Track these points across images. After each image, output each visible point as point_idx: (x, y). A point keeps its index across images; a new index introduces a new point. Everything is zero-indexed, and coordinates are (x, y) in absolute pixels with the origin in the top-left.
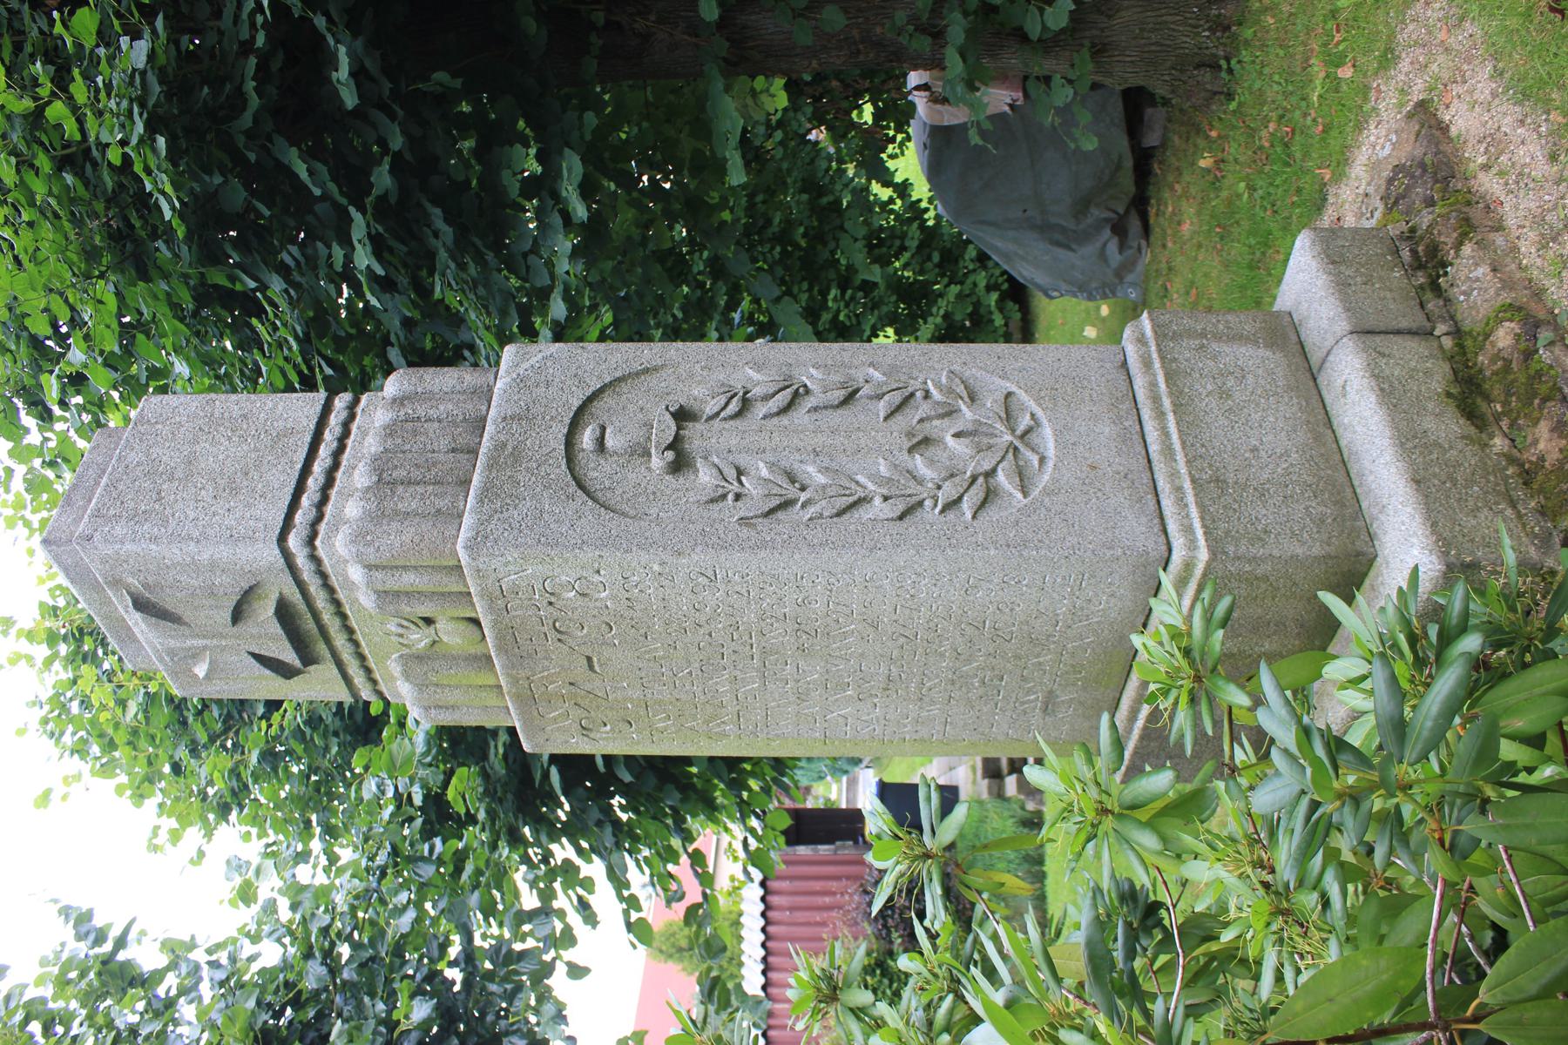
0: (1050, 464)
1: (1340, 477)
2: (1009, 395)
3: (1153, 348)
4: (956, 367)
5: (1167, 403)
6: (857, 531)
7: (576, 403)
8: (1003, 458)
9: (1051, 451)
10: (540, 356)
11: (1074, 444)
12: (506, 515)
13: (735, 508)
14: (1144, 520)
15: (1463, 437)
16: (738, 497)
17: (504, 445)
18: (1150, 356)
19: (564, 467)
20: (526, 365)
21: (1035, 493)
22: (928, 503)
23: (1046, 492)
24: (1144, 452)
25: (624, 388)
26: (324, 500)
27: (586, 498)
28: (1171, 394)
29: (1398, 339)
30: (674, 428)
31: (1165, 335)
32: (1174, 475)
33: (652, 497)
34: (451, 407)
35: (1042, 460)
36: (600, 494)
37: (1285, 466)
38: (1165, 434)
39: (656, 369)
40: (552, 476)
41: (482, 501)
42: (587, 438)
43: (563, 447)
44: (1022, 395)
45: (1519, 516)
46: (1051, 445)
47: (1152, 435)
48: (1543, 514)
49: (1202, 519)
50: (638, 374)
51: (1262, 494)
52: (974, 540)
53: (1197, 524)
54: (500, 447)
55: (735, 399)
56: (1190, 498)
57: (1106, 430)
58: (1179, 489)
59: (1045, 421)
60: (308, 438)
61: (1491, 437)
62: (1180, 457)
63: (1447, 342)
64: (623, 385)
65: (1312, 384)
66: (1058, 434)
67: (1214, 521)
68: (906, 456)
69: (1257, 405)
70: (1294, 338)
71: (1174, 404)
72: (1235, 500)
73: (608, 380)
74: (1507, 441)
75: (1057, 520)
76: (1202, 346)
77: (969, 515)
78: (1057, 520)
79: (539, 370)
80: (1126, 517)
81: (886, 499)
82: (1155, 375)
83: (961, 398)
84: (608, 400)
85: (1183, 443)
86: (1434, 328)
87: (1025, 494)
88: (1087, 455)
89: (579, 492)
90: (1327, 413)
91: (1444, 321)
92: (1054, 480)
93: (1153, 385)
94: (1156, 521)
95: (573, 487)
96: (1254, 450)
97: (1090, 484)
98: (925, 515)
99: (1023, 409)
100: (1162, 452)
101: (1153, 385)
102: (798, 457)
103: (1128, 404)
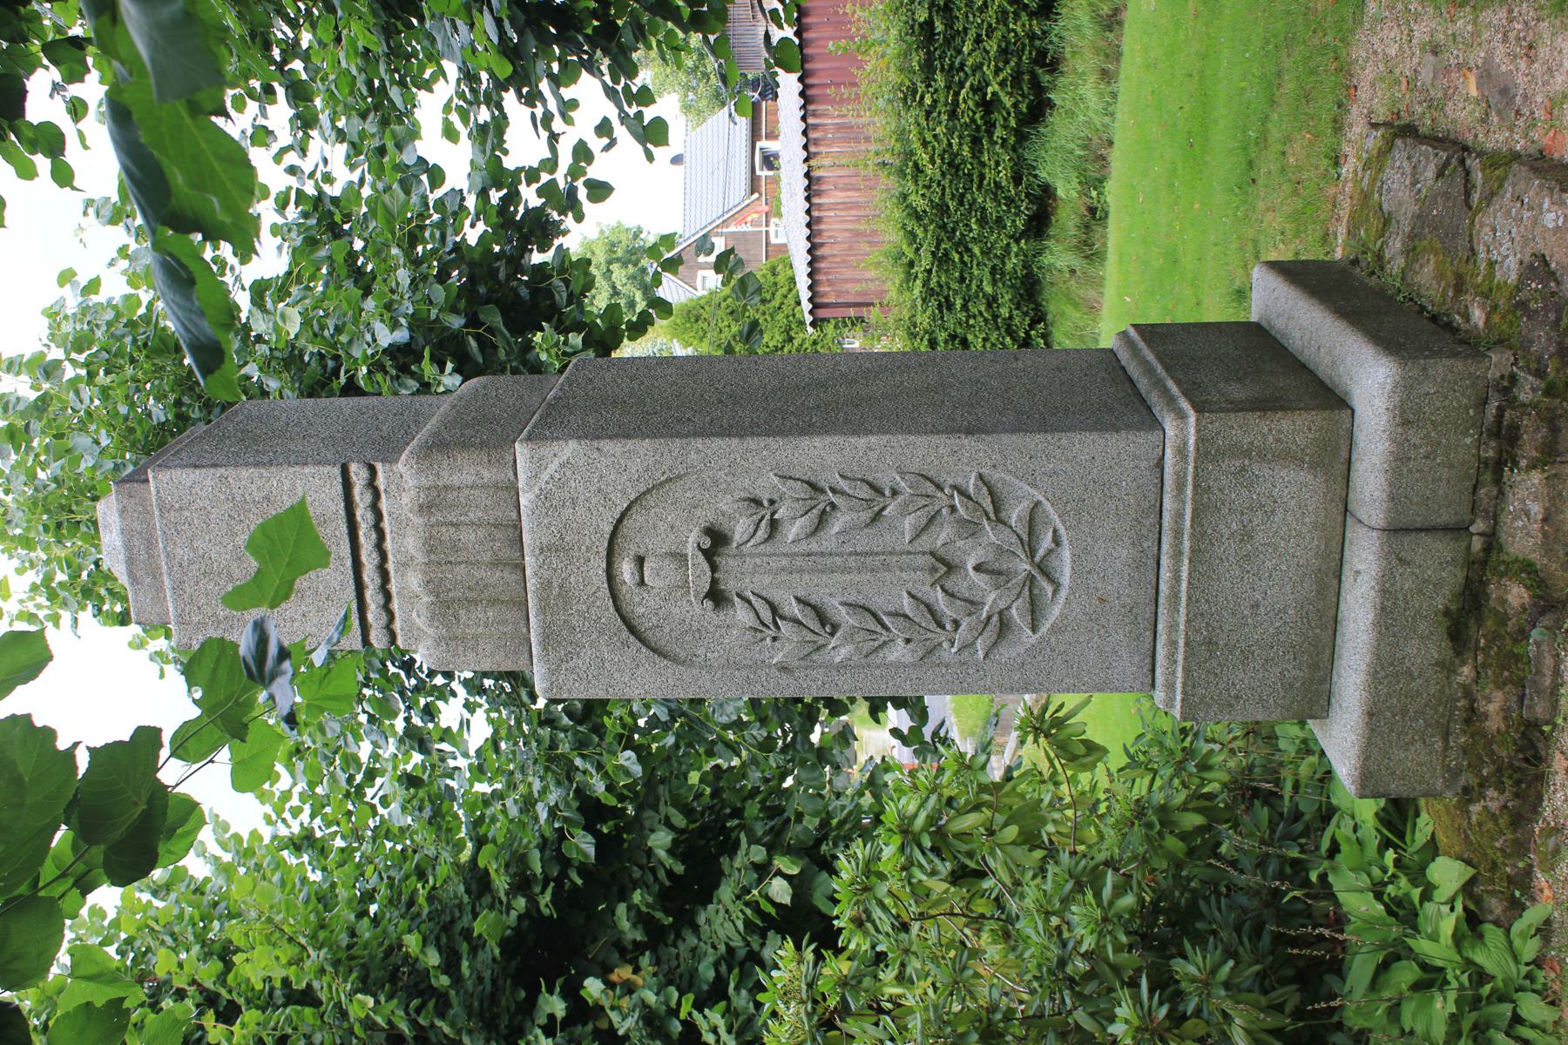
0: (1063, 593)
1: (1325, 637)
2: (1038, 504)
3: (1191, 469)
4: (984, 471)
5: (1187, 545)
6: (882, 676)
7: (608, 529)
8: (1018, 596)
9: (1066, 580)
10: (556, 461)
11: (1089, 572)
12: (572, 664)
13: (773, 647)
14: (1136, 659)
15: (1437, 664)
16: (774, 639)
17: (550, 583)
18: (1185, 474)
19: (612, 609)
20: (545, 476)
21: (1044, 628)
22: (945, 645)
23: (1054, 630)
24: (1154, 581)
25: (651, 500)
26: (387, 607)
27: (639, 644)
28: (1192, 536)
29: (1426, 539)
30: (709, 574)
31: (1207, 453)
32: (1173, 627)
33: (697, 636)
34: (480, 514)
35: (1055, 592)
36: (649, 635)
37: (1278, 624)
38: (1177, 578)
39: (679, 477)
40: (603, 620)
41: (545, 649)
42: (626, 570)
43: (606, 585)
44: (1047, 506)
45: (1446, 747)
46: (1067, 571)
47: (1165, 575)
48: (1465, 752)
49: (1184, 684)
50: (662, 484)
51: (1246, 656)
52: (982, 683)
53: (1179, 686)
54: (546, 585)
55: (764, 522)
56: (1180, 657)
57: (1124, 553)
58: (1174, 643)
59: (1066, 542)
60: (344, 529)
61: (1463, 663)
62: (1183, 610)
63: (1477, 544)
64: (649, 496)
65: (1340, 518)
66: (1076, 558)
67: (1194, 687)
68: (927, 588)
69: (1276, 549)
70: (1344, 454)
71: (1193, 551)
72: (1219, 665)
73: (632, 497)
74: (1473, 674)
75: (1059, 661)
76: (1243, 469)
77: (981, 654)
78: (1059, 661)
79: (561, 484)
80: (1121, 657)
81: (908, 641)
82: (1184, 502)
83: (987, 514)
84: (637, 519)
85: (1189, 598)
86: (1472, 522)
87: (1034, 629)
88: (1099, 585)
89: (632, 638)
90: (1341, 560)
91: (1486, 518)
92: (1063, 616)
93: (1179, 515)
94: (1148, 661)
95: (625, 633)
96: (1256, 606)
97: (1097, 619)
98: (942, 653)
99: (1048, 522)
100: (1169, 598)
101: (1179, 515)
102: (827, 591)
103: (1153, 519)
